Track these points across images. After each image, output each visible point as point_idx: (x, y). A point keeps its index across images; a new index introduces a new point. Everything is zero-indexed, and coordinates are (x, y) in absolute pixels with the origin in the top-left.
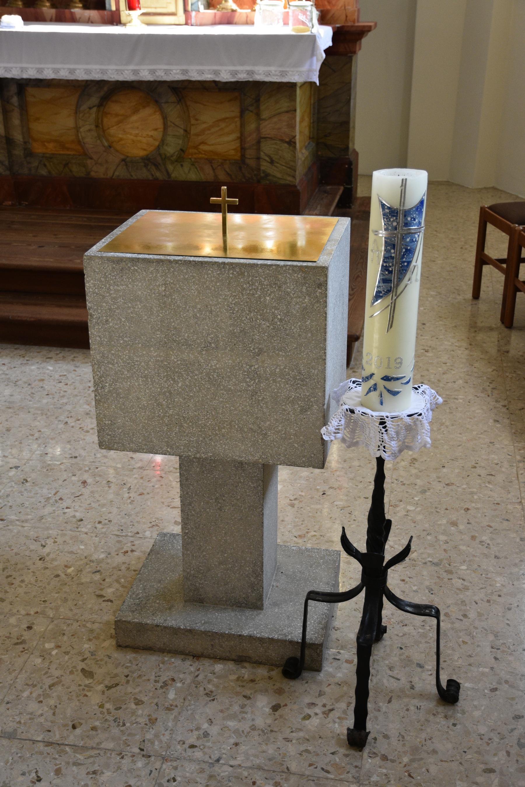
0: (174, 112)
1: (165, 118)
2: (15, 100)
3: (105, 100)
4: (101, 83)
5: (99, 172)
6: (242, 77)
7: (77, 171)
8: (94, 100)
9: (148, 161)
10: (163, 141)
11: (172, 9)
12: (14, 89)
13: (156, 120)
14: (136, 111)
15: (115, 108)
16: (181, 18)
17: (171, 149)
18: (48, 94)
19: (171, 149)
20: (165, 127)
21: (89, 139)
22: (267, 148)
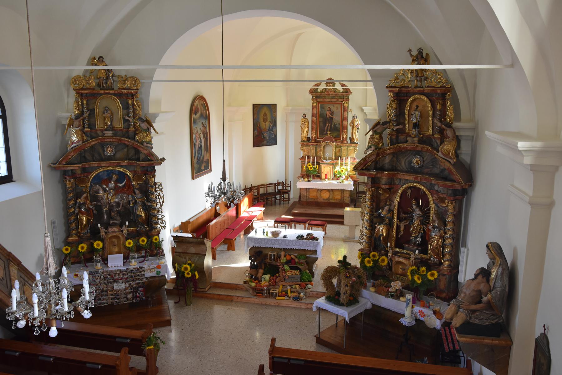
0: (331, 193)
5: (319, 201)
7: (316, 200)
9: (327, 199)
15: (322, 192)
17: (331, 198)
19: (331, 198)
21: (318, 196)
22: (345, 198)
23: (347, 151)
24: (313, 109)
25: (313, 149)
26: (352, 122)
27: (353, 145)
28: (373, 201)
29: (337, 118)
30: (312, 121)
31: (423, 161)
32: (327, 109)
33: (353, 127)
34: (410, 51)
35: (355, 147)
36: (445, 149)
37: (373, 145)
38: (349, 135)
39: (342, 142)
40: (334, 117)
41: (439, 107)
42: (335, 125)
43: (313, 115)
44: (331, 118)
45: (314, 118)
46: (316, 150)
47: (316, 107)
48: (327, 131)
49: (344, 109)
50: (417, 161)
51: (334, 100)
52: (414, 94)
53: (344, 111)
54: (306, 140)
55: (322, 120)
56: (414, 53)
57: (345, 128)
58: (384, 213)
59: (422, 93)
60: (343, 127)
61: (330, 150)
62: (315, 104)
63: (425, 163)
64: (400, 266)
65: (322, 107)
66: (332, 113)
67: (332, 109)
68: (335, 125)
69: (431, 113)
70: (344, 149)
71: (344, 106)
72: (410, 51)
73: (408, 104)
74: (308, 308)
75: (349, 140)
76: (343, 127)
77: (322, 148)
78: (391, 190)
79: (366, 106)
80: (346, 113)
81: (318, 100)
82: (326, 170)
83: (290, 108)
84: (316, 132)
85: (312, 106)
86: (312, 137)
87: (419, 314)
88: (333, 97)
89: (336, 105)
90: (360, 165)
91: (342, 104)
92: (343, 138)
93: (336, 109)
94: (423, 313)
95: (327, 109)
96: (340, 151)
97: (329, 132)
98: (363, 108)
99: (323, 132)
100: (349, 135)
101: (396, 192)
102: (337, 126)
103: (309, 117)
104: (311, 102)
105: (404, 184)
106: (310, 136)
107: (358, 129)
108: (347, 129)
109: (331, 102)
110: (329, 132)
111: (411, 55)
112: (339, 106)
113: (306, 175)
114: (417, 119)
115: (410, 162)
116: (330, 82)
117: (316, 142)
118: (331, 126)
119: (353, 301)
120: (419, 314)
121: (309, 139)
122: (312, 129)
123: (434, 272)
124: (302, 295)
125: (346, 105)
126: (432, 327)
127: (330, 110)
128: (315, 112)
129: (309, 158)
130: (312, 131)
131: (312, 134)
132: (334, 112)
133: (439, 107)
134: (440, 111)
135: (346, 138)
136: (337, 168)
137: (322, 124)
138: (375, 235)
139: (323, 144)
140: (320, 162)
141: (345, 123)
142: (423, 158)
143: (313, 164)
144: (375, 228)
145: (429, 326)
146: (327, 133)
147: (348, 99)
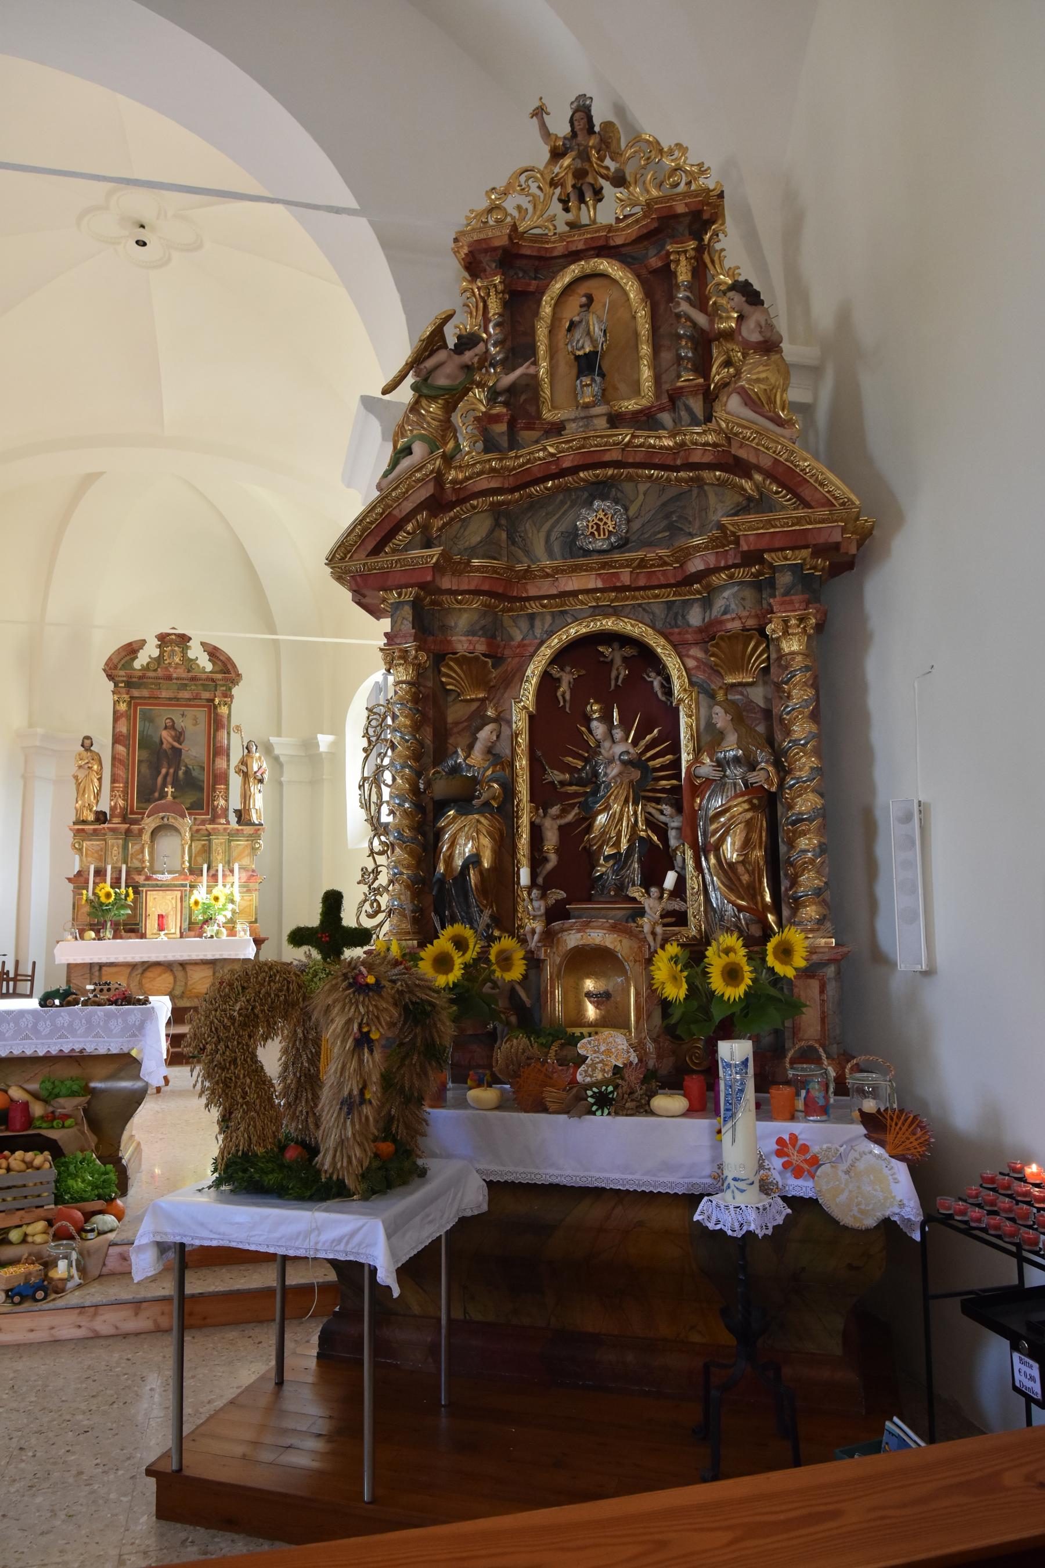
0: (180, 974)
1: (175, 978)
2: (97, 973)
3: (145, 971)
4: (143, 963)
6: (217, 957)
8: (140, 971)
10: (173, 989)
11: (173, 931)
12: (97, 968)
13: (171, 979)
14: (160, 975)
15: (149, 974)
16: (178, 935)
18: (113, 970)
20: (175, 981)
23: (229, 850)
24: (116, 720)
25: (115, 844)
26: (243, 762)
27: (248, 830)
28: (423, 715)
29: (194, 751)
30: (114, 758)
31: (629, 521)
32: (162, 722)
33: (246, 775)
34: (539, 112)
35: (255, 837)
36: (749, 381)
37: (422, 438)
38: (235, 802)
39: (213, 821)
40: (184, 747)
41: (683, 274)
42: (188, 772)
43: (117, 739)
44: (177, 752)
45: (121, 748)
46: (125, 847)
47: (126, 715)
48: (164, 785)
49: (217, 723)
50: (598, 520)
51: (186, 694)
52: (574, 256)
53: (216, 730)
54: (91, 817)
55: (145, 755)
56: (560, 126)
57: (223, 778)
58: (474, 760)
59: (604, 250)
60: (215, 776)
61: (174, 850)
62: (123, 707)
63: (636, 525)
64: (589, 984)
65: (148, 718)
66: (179, 737)
67: (180, 723)
68: (188, 772)
69: (644, 328)
70: (218, 842)
71: (216, 714)
72: (539, 112)
73: (546, 310)
74: (97, 1336)
75: (233, 818)
76: (215, 776)
77: (146, 837)
78: (496, 669)
79: (279, 735)
80: (223, 734)
81: (136, 693)
82: (159, 904)
83: (40, 730)
84: (125, 792)
85: (115, 712)
86: (113, 809)
87: (777, 1163)
88: (184, 687)
89: (191, 712)
90: (362, 539)
91: (211, 707)
92: (214, 809)
93: (192, 723)
94: (804, 1149)
95: (162, 722)
96: (207, 851)
97: (169, 790)
98: (273, 740)
99: (148, 794)
100: (235, 802)
101: (517, 675)
102: (195, 774)
103: (104, 745)
104: (109, 699)
105: (551, 634)
106: (104, 806)
107: (261, 781)
108: (227, 783)
109: (174, 702)
110: (169, 790)
111: (546, 133)
112: (201, 714)
113: (95, 919)
114: (593, 341)
115: (573, 534)
116: (174, 642)
117: (125, 819)
118: (176, 773)
119: (391, 1168)
120: (777, 1163)
121: (101, 817)
122: (114, 780)
123: (739, 991)
124: (61, 1269)
125: (223, 710)
126: (870, 1222)
127: (173, 727)
128: (123, 728)
129: (100, 873)
130: (112, 790)
131: (112, 797)
132: (187, 735)
133: (683, 274)
134: (689, 288)
135: (227, 809)
136: (200, 894)
137: (145, 769)
138: (441, 868)
139: (150, 823)
140: (140, 879)
141: (221, 763)
142: (626, 509)
143: (116, 883)
144: (438, 834)
145: (847, 1219)
146: (163, 795)
147: (228, 695)
